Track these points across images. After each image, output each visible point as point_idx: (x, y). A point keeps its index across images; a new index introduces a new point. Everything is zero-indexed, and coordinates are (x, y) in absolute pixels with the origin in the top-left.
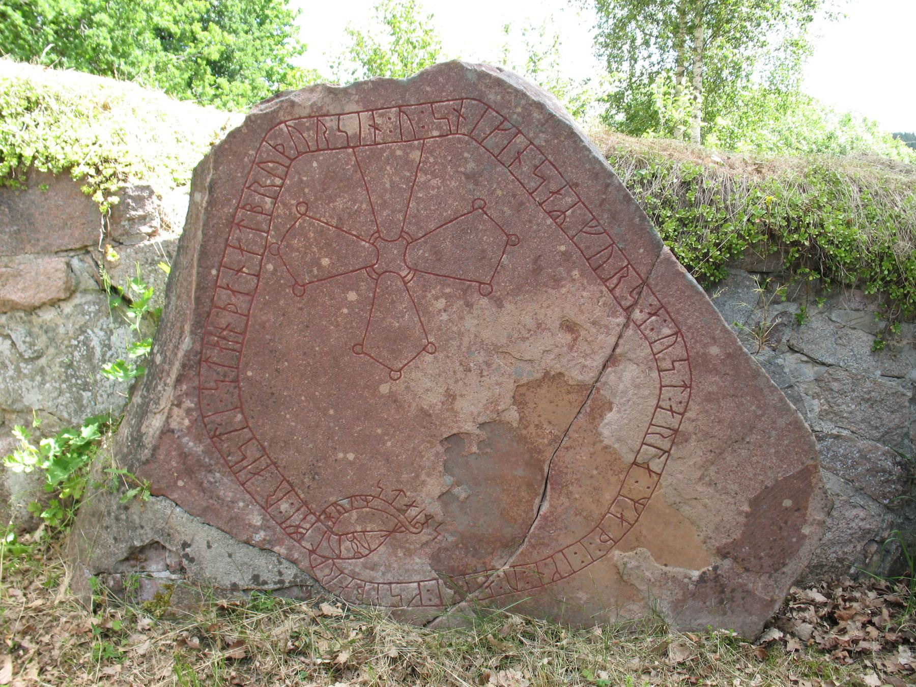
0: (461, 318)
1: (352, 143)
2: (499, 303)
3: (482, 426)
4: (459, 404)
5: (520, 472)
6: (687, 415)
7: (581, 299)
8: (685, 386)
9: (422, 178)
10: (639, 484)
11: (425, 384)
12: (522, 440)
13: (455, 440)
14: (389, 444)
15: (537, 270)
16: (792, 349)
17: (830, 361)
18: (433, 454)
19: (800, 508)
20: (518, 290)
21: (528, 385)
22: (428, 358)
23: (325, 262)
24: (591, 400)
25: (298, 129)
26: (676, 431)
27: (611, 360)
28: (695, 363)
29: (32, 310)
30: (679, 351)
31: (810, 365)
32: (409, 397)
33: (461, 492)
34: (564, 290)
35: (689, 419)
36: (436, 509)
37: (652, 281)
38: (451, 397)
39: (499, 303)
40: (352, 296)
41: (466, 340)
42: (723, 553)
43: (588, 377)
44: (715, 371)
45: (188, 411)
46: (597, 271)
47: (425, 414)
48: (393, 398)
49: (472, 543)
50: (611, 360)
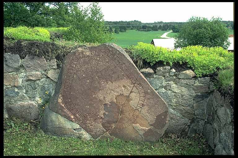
0: (106, 85)
3: (110, 102)
7: (126, 82)
8: (144, 97)
10: (137, 113)
11: (100, 96)
13: (106, 105)
16: (170, 90)
17: (177, 92)
19: (165, 117)
21: (117, 96)
23: (84, 75)
24: (128, 98)
25: (79, 54)
28: (146, 93)
29: (35, 81)
30: (143, 91)
32: (98, 97)
33: (107, 113)
36: (102, 116)
38: (104, 98)
39: (113, 83)
40: (88, 81)
42: (151, 125)
43: (128, 95)
45: (62, 99)
46: (128, 77)
48: (95, 97)
49: (109, 122)
50: (131, 92)
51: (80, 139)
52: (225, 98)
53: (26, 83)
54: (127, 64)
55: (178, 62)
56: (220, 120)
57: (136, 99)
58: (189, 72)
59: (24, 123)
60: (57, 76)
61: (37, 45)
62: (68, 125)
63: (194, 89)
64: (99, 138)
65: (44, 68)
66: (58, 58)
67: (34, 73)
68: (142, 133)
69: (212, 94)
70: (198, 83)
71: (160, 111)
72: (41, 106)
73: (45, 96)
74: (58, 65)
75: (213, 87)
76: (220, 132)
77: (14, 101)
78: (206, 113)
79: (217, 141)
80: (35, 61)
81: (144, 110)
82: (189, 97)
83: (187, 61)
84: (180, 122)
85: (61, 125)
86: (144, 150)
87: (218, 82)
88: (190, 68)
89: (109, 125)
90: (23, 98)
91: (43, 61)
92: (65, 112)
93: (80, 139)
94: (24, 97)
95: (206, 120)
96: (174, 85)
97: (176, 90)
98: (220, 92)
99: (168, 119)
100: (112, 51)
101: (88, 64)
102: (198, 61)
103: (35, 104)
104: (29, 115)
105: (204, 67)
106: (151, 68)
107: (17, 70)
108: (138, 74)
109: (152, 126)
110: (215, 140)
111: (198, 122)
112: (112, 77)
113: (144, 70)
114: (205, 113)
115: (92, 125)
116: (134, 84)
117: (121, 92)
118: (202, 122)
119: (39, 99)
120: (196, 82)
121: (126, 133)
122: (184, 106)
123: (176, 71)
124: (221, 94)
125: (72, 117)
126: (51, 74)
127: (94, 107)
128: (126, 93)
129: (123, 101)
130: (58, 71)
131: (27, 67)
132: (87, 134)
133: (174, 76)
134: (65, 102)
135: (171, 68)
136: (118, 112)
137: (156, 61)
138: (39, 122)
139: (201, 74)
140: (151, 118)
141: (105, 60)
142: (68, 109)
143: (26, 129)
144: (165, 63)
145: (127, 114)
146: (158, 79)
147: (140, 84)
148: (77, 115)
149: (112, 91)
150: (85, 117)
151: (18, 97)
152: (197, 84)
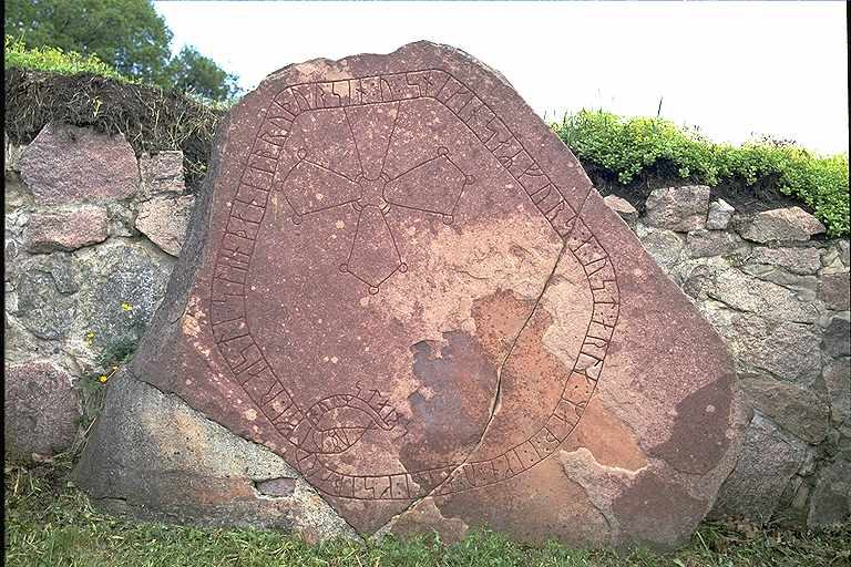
1: (344, 103)
2: (459, 232)
3: (445, 334)
4: (427, 315)
5: (477, 376)
6: (617, 327)
7: (527, 228)
8: (614, 303)
10: (580, 388)
11: (397, 298)
12: (478, 347)
13: (423, 347)
14: (367, 349)
15: (490, 204)
16: (710, 297)
18: (404, 359)
21: (483, 300)
22: (401, 276)
23: (319, 197)
24: (536, 312)
25: (302, 92)
26: (608, 342)
28: (623, 283)
29: (72, 251)
30: (608, 273)
31: (727, 311)
32: (384, 309)
33: (428, 392)
34: (511, 221)
35: (619, 331)
36: (405, 407)
38: (418, 309)
39: (459, 232)
40: (340, 224)
41: (432, 261)
42: (653, 453)
43: (534, 293)
44: (639, 290)
45: (200, 320)
46: (538, 205)
47: (397, 324)
48: (371, 310)
49: (438, 442)
55: (739, 177)
58: (793, 214)
60: (177, 227)
62: (228, 459)
64: (387, 529)
65: (123, 188)
67: (71, 209)
68: (605, 496)
70: (838, 262)
71: (694, 376)
72: (88, 377)
73: (118, 328)
74: (188, 179)
80: (83, 154)
81: (616, 375)
82: (800, 332)
84: (767, 457)
85: (191, 459)
88: (794, 200)
89: (436, 457)
91: (117, 156)
92: (213, 389)
96: (730, 274)
97: (739, 297)
100: (460, 77)
101: (341, 138)
103: (60, 369)
104: (27, 424)
109: (659, 457)
112: (457, 202)
115: (349, 460)
116: (565, 237)
117: (499, 280)
119: (83, 345)
120: (831, 256)
121: (523, 500)
122: (779, 379)
125: (251, 415)
127: (364, 360)
128: (525, 285)
129: (508, 325)
130: (189, 201)
132: (324, 507)
133: (727, 230)
134: (217, 337)
135: (713, 198)
136: (485, 388)
138: (75, 460)
140: (650, 416)
141: (426, 117)
142: (234, 373)
144: (684, 173)
145: (530, 396)
147: (593, 239)
148: (276, 404)
150: (316, 419)
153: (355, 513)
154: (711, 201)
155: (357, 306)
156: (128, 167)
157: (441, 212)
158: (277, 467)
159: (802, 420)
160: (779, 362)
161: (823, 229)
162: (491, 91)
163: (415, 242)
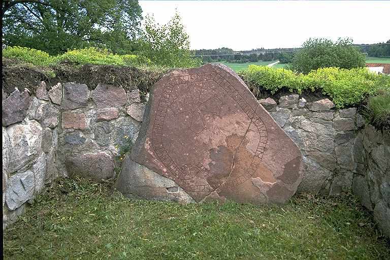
2: (221, 118)
3: (218, 147)
4: (213, 141)
5: (228, 158)
7: (241, 116)
9: (203, 90)
10: (257, 160)
11: (204, 137)
13: (212, 150)
15: (230, 110)
16: (299, 128)
17: (310, 131)
20: (225, 114)
21: (229, 137)
26: (265, 148)
27: (248, 131)
28: (268, 131)
29: (109, 121)
33: (214, 163)
36: (208, 167)
37: (257, 112)
38: (210, 140)
39: (221, 118)
40: (187, 117)
42: (278, 178)
43: (243, 134)
44: (273, 133)
46: (243, 110)
48: (197, 140)
49: (217, 176)
50: (248, 131)
51: (177, 202)
52: (382, 132)
53: (96, 124)
54: (241, 91)
55: (310, 89)
56: (378, 166)
57: (254, 141)
58: (326, 102)
59: (91, 183)
61: (112, 71)
63: (333, 126)
66: (142, 88)
67: (108, 109)
68: (264, 190)
69: (361, 132)
71: (289, 156)
72: (116, 158)
74: (141, 97)
75: (361, 120)
76: (379, 184)
77: (77, 151)
78: (353, 160)
79: (375, 198)
81: (268, 156)
83: (322, 87)
84: (317, 175)
85: (149, 183)
86: (271, 215)
87: (369, 112)
88: (327, 96)
89: (217, 180)
90: (90, 146)
91: (121, 92)
93: (177, 202)
94: (93, 146)
95: (355, 171)
96: (305, 121)
98: (374, 125)
99: (302, 168)
102: (336, 87)
103: (108, 155)
104: (99, 170)
105: (345, 93)
106: (272, 98)
107: (84, 105)
108: (257, 104)
110: (373, 197)
111: (343, 174)
113: (262, 100)
114: (352, 160)
115: (193, 182)
117: (233, 131)
118: (349, 175)
121: (242, 191)
122: (321, 151)
123: (307, 101)
124: (376, 128)
125: (165, 170)
126: (132, 110)
128: (240, 133)
131: (99, 101)
132: (186, 194)
135: (300, 97)
137: (278, 88)
139: (343, 103)
142: (160, 159)
143: (96, 191)
144: (291, 91)
145: (242, 163)
146: (283, 112)
147: (260, 119)
148: (172, 167)
149: (222, 130)
150: (183, 169)
151: (84, 146)
152: (338, 118)
153: (195, 196)
154: (299, 99)
155: (193, 139)
156: (124, 96)
157: (216, 112)
158: (173, 184)
159: (328, 164)
160: (321, 147)
161: (335, 106)
162: (229, 78)
163: (208, 121)
